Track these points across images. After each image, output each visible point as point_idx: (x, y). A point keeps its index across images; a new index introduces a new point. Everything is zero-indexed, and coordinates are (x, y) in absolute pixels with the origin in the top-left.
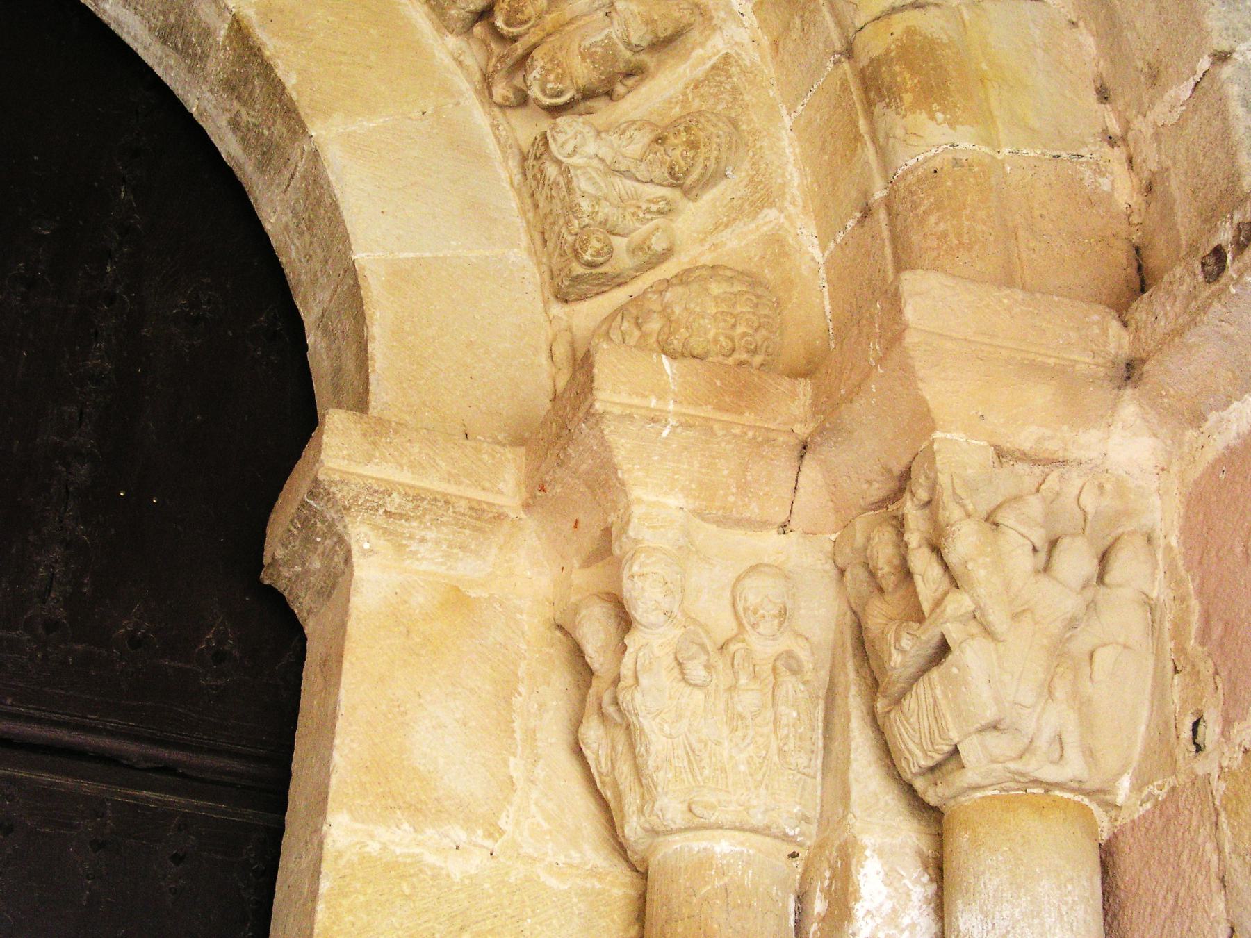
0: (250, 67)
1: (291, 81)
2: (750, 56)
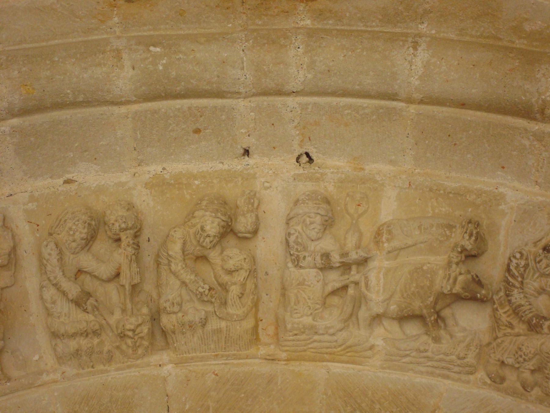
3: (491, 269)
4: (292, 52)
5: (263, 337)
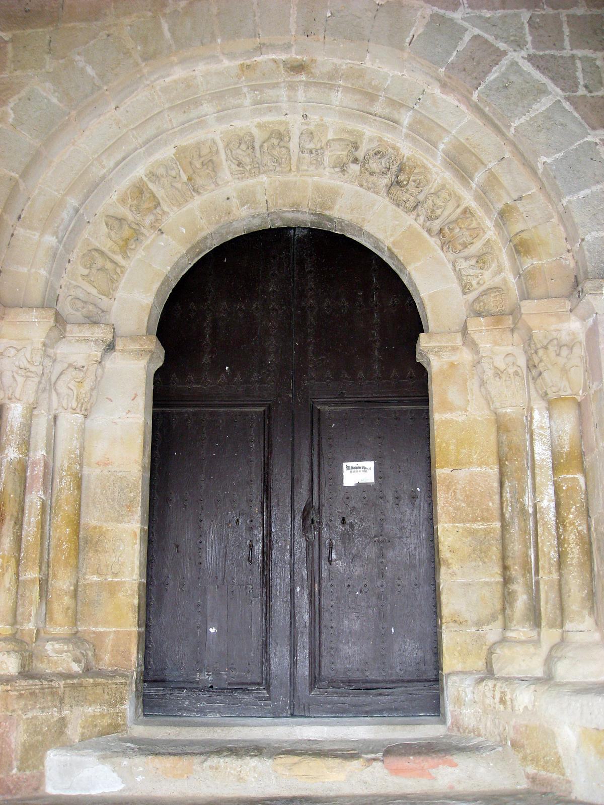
0: (392, 255)
1: (401, 259)
2: (494, 238)
3: (360, 154)
4: (299, 92)
5: (293, 169)
